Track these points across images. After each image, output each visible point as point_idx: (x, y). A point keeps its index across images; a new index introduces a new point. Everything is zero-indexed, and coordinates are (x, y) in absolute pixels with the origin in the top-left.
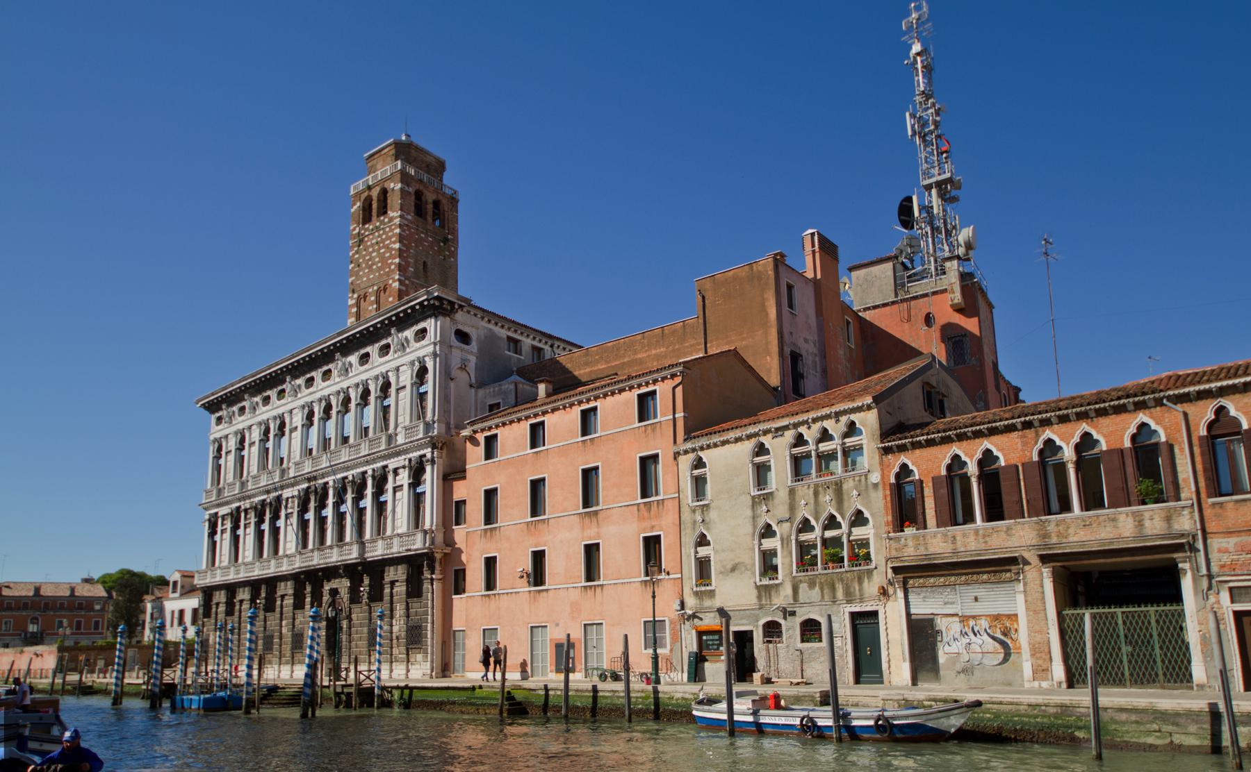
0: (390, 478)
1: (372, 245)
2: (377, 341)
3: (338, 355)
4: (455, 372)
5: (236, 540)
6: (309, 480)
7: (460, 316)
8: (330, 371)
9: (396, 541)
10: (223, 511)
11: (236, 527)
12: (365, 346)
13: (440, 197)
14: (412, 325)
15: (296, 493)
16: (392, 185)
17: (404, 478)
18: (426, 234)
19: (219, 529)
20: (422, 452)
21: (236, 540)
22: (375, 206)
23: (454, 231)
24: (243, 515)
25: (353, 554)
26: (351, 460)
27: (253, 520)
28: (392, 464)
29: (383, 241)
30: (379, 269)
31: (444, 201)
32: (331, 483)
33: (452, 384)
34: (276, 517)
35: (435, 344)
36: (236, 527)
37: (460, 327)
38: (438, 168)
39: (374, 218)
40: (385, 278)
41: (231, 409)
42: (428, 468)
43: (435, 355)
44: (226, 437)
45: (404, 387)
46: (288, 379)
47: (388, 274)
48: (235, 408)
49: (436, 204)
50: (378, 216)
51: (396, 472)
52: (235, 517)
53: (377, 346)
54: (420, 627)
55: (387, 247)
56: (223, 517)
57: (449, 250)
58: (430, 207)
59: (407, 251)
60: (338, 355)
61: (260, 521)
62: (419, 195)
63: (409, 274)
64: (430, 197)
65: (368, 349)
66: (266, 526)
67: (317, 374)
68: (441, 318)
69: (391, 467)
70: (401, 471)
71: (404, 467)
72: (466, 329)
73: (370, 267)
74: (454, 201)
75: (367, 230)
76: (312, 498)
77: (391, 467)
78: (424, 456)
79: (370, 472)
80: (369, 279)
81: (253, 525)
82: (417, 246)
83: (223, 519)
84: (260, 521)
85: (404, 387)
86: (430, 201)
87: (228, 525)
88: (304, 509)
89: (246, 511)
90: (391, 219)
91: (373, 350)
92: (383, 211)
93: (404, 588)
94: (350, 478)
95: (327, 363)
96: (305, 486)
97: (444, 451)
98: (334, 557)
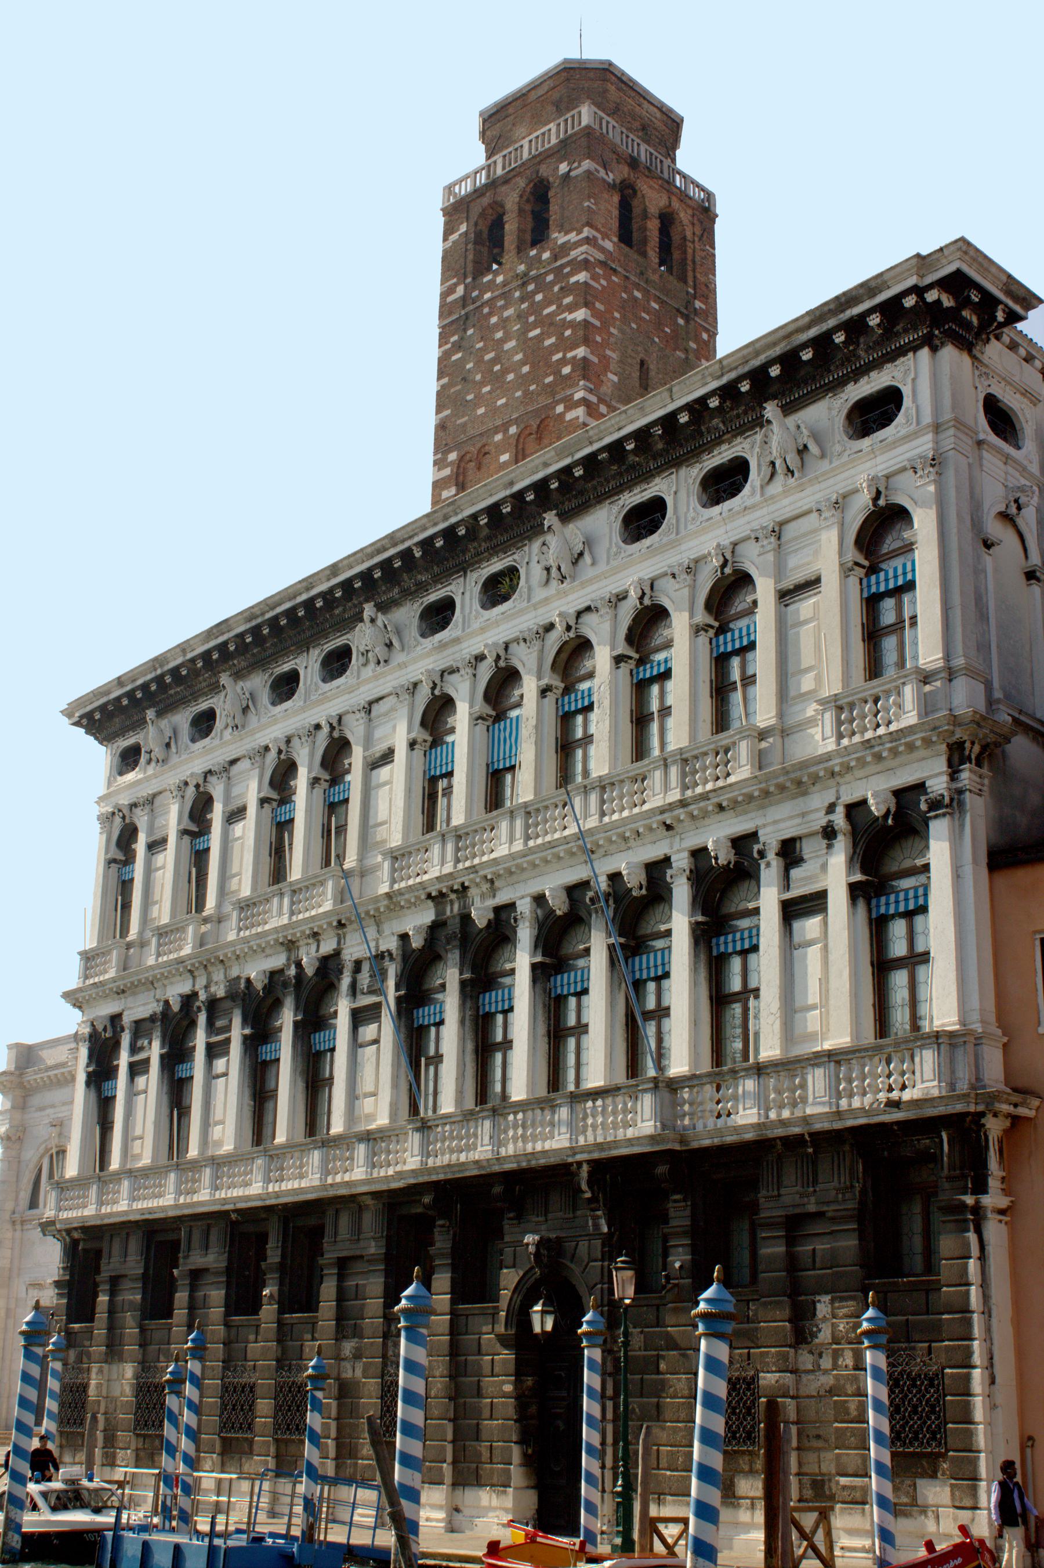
0: (770, 873)
1: (504, 322)
2: (693, 455)
3: (550, 518)
4: (995, 529)
5: (177, 1092)
6: (438, 899)
7: (994, 351)
8: (512, 572)
9: (817, 1080)
10: (140, 1007)
11: (177, 1055)
12: (647, 476)
13: (676, 204)
14: (840, 384)
15: (391, 944)
16: (563, 168)
17: (834, 871)
18: (646, 292)
19: (124, 1060)
20: (905, 778)
21: (177, 1092)
22: (511, 227)
23: (707, 292)
24: (202, 1018)
25: (639, 1124)
26: (625, 814)
27: (237, 1032)
28: (774, 826)
29: (536, 309)
30: (523, 381)
31: (684, 216)
32: (524, 907)
33: (988, 561)
34: (314, 1022)
35: (937, 428)
36: (177, 1055)
37: (997, 390)
38: (667, 129)
39: (509, 256)
40: (544, 401)
41: (164, 723)
42: (939, 831)
43: (936, 462)
44: (151, 800)
45: (812, 584)
46: (369, 610)
47: (550, 390)
48: (182, 719)
49: (667, 220)
50: (520, 250)
51: (790, 853)
52: (175, 1027)
53: (692, 475)
54: (935, 1380)
55: (550, 325)
56: (140, 1028)
57: (697, 339)
58: (653, 226)
59: (605, 325)
60: (550, 518)
61: (261, 1035)
62: (627, 193)
63: (606, 389)
64: (653, 200)
65: (657, 487)
66: (285, 1049)
67: (465, 591)
68: (949, 353)
69: (770, 838)
70: (809, 849)
71: (829, 833)
72: (1010, 399)
73: (497, 379)
74: (705, 213)
75: (491, 286)
76: (453, 957)
77: (770, 838)
78: (920, 787)
79: (681, 861)
80: (494, 411)
81: (236, 1048)
82: (624, 319)
83: (136, 1035)
84: (261, 1035)
85: (812, 584)
86: (653, 210)
87: (155, 1051)
88: (416, 995)
89: (213, 1006)
90: (566, 248)
91: (678, 488)
92: (538, 231)
93: (851, 1242)
94: (603, 884)
95: (496, 550)
96: (427, 916)
97: (985, 771)
98: (554, 1139)
